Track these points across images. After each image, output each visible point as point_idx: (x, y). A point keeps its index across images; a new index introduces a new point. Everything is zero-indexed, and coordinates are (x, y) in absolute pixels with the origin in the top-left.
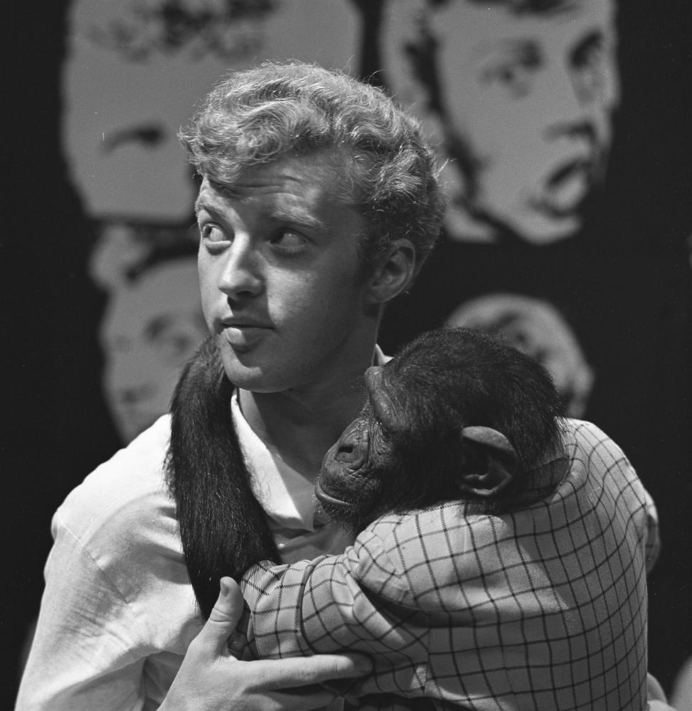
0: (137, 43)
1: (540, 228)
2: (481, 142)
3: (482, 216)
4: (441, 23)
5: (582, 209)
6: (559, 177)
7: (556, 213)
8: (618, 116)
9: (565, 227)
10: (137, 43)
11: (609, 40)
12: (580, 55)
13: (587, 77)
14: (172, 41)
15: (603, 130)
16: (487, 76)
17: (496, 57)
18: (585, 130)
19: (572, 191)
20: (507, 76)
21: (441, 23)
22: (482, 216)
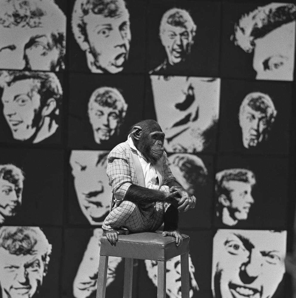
0: (6, 24)
1: (114, 70)
2: (98, 50)
3: (99, 67)
4: (87, 19)
5: (123, 65)
6: (118, 58)
7: (118, 67)
8: (131, 43)
9: (121, 69)
10: (6, 24)
11: (128, 23)
12: (121, 28)
13: (123, 32)
14: (17, 23)
15: (128, 46)
16: (99, 33)
17: (101, 28)
18: (124, 46)
19: (121, 61)
20: (104, 33)
21: (87, 19)
22: (99, 67)
